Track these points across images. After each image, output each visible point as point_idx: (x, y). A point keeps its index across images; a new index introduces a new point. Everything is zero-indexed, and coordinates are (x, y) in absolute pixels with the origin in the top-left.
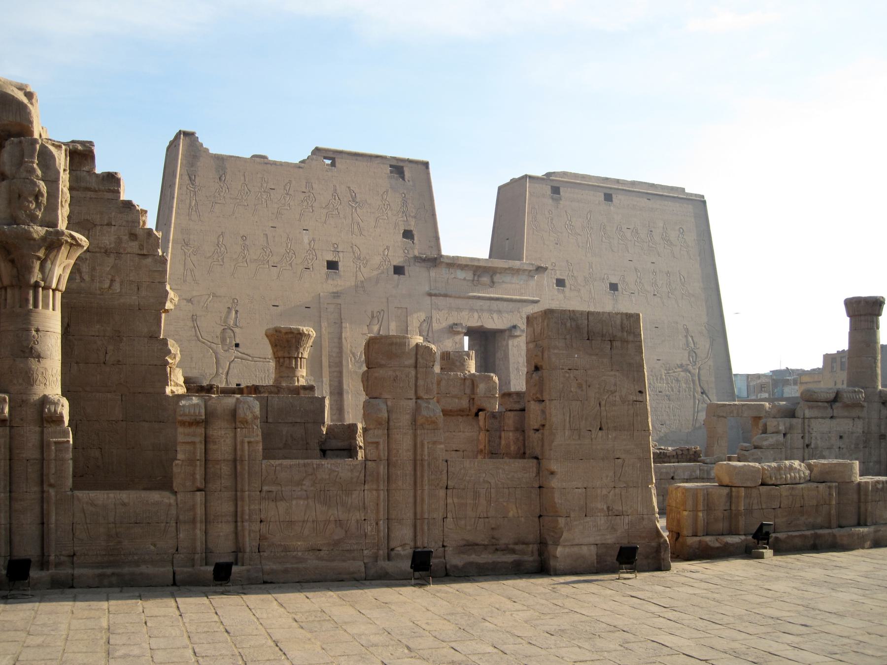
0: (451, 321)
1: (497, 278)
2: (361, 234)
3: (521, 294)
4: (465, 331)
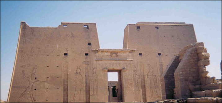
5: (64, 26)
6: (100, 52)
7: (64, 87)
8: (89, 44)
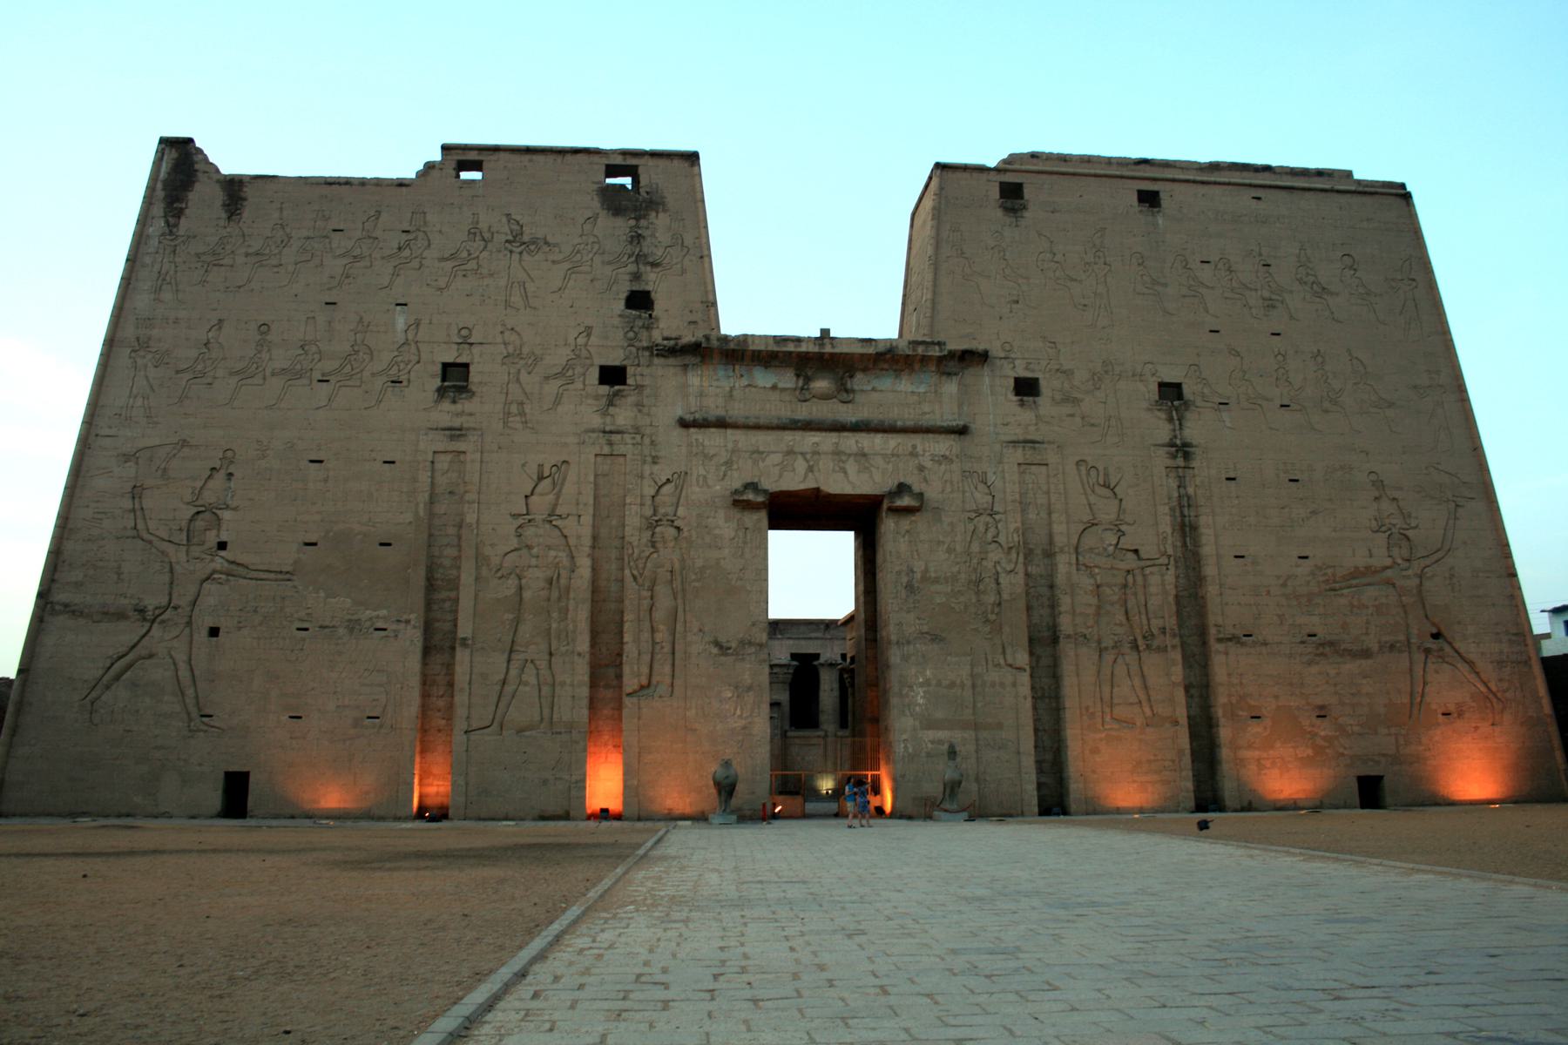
1: (860, 381)
4: (760, 499)
5: (464, 175)
7: (428, 628)
8: (640, 301)
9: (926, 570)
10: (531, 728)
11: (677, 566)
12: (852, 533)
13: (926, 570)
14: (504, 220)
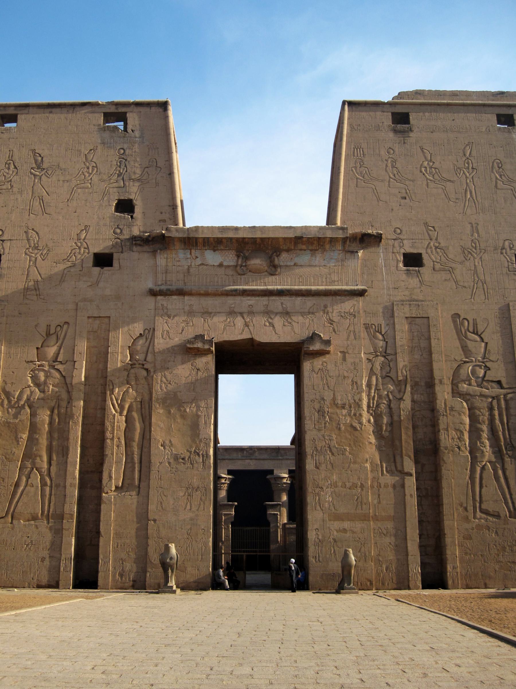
0: (190, 333)
1: (284, 258)
2: (44, 212)
3: (332, 282)
4: (207, 347)
6: (178, 245)
8: (125, 206)
9: (334, 399)
10: (34, 518)
11: (147, 398)
12: (293, 375)
13: (334, 399)
14: (31, 153)
